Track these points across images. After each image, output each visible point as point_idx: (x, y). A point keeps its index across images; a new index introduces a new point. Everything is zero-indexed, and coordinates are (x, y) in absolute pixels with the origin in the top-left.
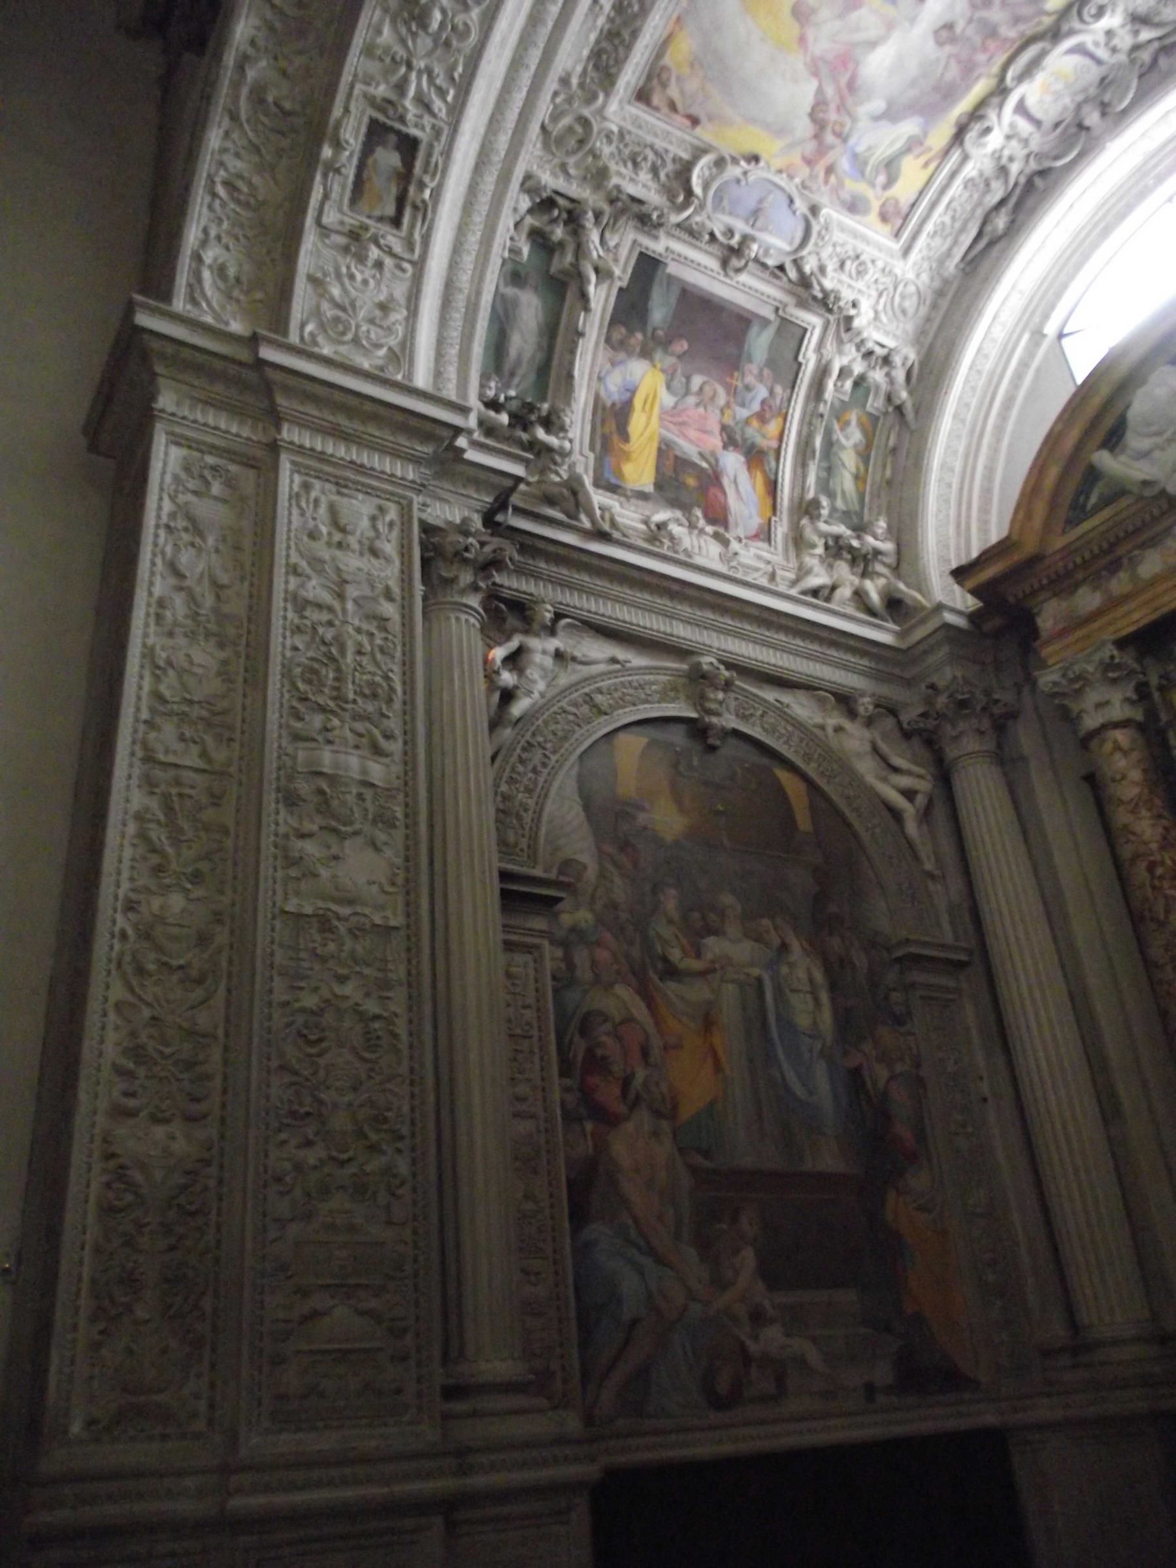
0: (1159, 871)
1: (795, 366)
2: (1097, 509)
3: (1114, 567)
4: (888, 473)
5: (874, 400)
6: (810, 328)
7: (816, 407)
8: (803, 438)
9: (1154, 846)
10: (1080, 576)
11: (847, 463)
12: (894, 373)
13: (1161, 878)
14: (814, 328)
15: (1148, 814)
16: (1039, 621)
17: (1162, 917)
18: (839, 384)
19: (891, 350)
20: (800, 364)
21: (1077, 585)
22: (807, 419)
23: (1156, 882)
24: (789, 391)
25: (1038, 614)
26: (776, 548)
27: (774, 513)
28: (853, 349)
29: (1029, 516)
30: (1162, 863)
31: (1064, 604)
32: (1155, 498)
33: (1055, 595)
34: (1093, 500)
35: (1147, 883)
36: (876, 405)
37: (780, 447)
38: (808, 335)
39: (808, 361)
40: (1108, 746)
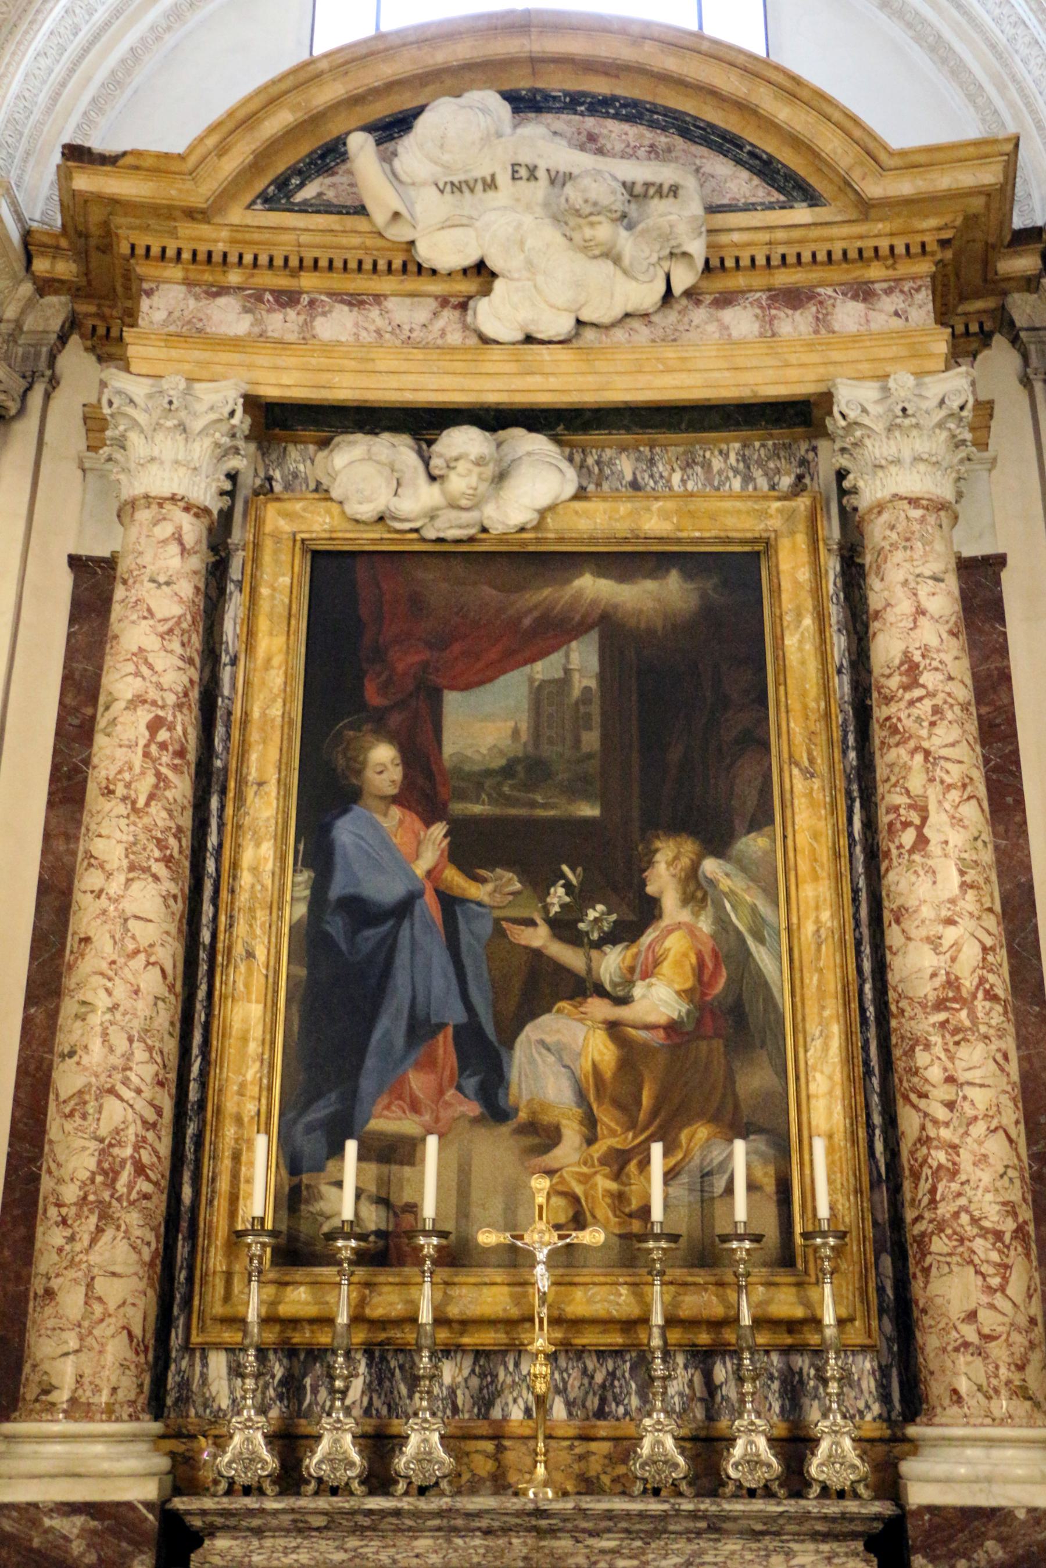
0: (163, 735)
2: (304, 208)
3: (287, 299)
9: (171, 699)
10: (234, 277)
13: (163, 746)
15: (179, 650)
16: (145, 303)
17: (141, 803)
21: (222, 291)
23: (154, 749)
25: (149, 293)
29: (222, 150)
30: (171, 728)
31: (192, 303)
32: (395, 246)
33: (189, 283)
34: (309, 192)
35: (142, 742)
40: (165, 530)
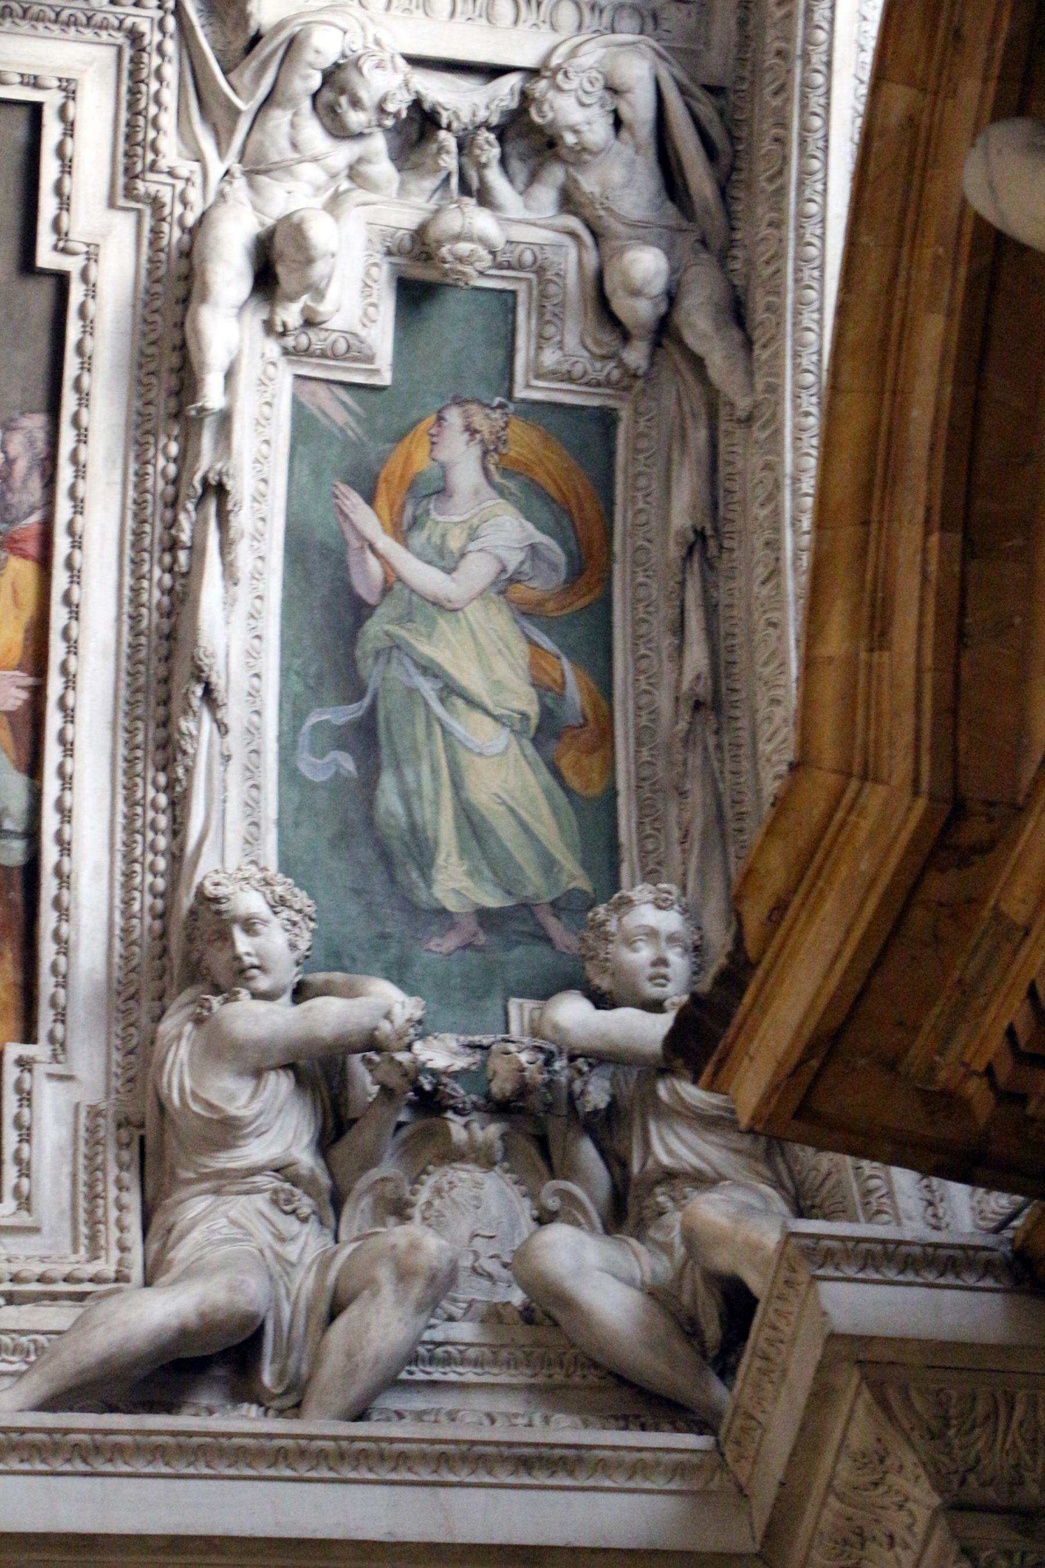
1: (41, 294)
4: (696, 657)
5: (541, 340)
6: (51, 100)
7: (185, 459)
8: (150, 619)
11: (471, 678)
12: (589, 183)
14: (69, 89)
18: (290, 314)
19: (533, 73)
20: (61, 280)
22: (154, 532)
24: (36, 423)
26: (25, 1202)
27: (29, 1036)
28: (312, 132)
36: (550, 358)
37: (38, 694)
38: (52, 132)
39: (92, 255)
